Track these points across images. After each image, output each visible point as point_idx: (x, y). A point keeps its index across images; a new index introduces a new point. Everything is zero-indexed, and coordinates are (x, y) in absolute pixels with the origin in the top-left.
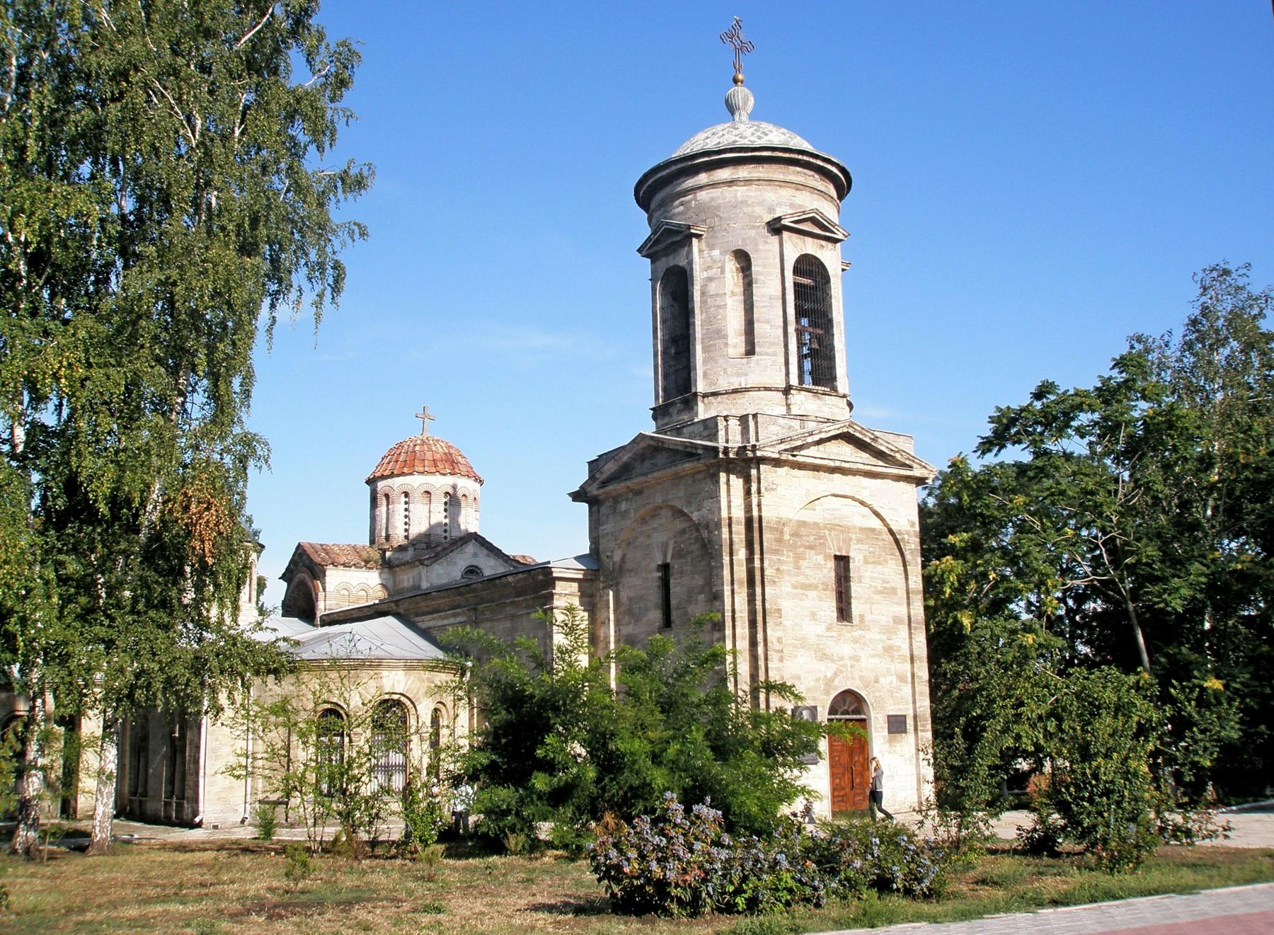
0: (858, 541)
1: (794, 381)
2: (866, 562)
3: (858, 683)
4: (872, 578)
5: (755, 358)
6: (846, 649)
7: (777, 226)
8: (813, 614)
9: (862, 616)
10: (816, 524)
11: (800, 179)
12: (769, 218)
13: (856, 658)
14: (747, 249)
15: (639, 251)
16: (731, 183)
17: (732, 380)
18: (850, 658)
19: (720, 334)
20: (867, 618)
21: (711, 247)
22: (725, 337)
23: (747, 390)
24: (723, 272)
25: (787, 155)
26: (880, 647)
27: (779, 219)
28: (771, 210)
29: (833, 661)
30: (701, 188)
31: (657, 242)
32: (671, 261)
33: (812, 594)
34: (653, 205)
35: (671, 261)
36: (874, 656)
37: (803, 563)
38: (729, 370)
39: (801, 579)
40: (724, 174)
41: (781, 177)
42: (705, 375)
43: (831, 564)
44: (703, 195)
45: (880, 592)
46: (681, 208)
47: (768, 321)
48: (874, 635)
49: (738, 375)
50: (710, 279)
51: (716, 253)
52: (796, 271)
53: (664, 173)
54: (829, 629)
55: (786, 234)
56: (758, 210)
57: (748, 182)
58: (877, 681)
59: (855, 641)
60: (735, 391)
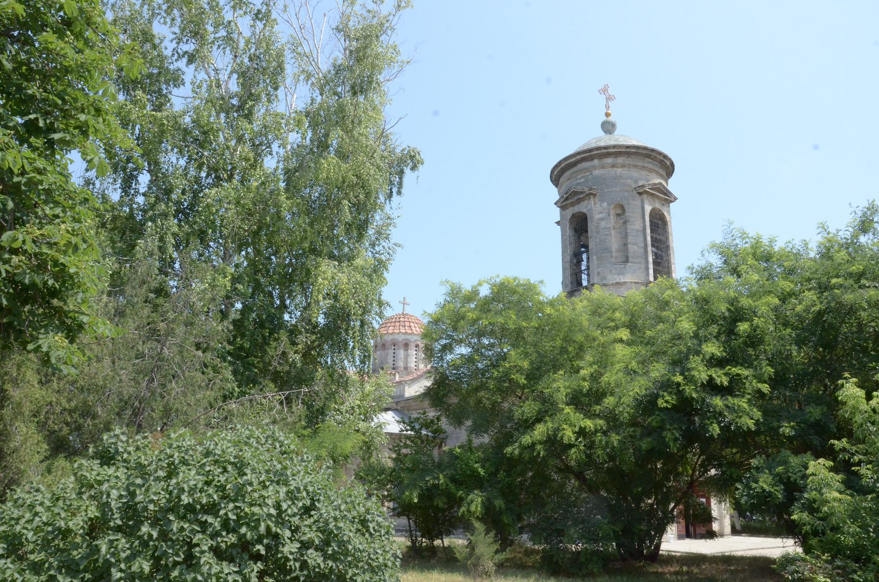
1: (651, 278)
5: (629, 264)
7: (641, 191)
11: (651, 166)
12: (634, 186)
14: (624, 203)
15: (556, 204)
16: (613, 166)
17: (615, 277)
19: (608, 250)
21: (602, 201)
22: (611, 252)
23: (625, 283)
24: (609, 215)
25: (645, 152)
27: (643, 186)
28: (636, 181)
30: (595, 168)
31: (567, 199)
32: (576, 209)
34: (561, 180)
35: (576, 209)
38: (614, 272)
40: (609, 160)
41: (640, 164)
42: (599, 273)
44: (596, 172)
46: (582, 180)
47: (635, 244)
49: (619, 274)
50: (602, 219)
51: (605, 204)
52: (650, 216)
53: (572, 160)
55: (645, 196)
56: (629, 181)
57: (623, 166)
60: (618, 283)
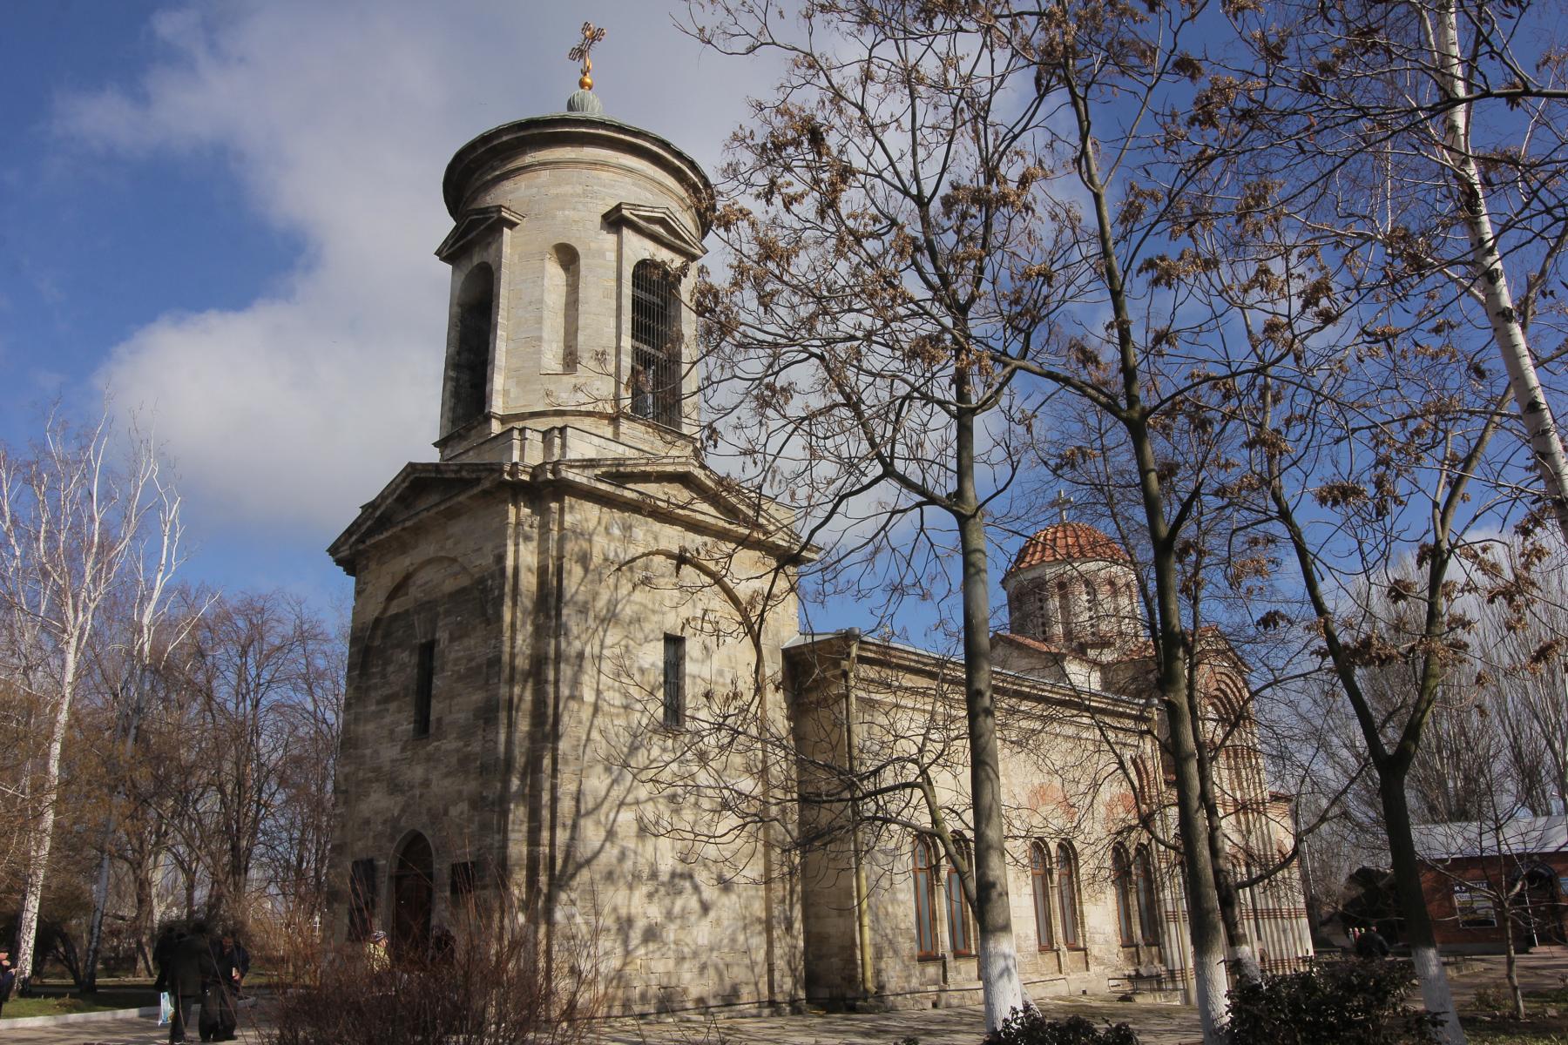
0: (448, 613)
2: (452, 639)
3: (425, 819)
4: (456, 661)
6: (418, 772)
8: (392, 732)
9: (439, 720)
10: (407, 611)
13: (426, 783)
18: (422, 784)
20: (447, 719)
26: (454, 760)
29: (403, 792)
33: (393, 706)
36: (447, 775)
37: (391, 669)
39: (386, 691)
43: (415, 660)
45: (460, 678)
48: (450, 744)
54: (403, 749)
58: (446, 813)
59: (429, 758)
